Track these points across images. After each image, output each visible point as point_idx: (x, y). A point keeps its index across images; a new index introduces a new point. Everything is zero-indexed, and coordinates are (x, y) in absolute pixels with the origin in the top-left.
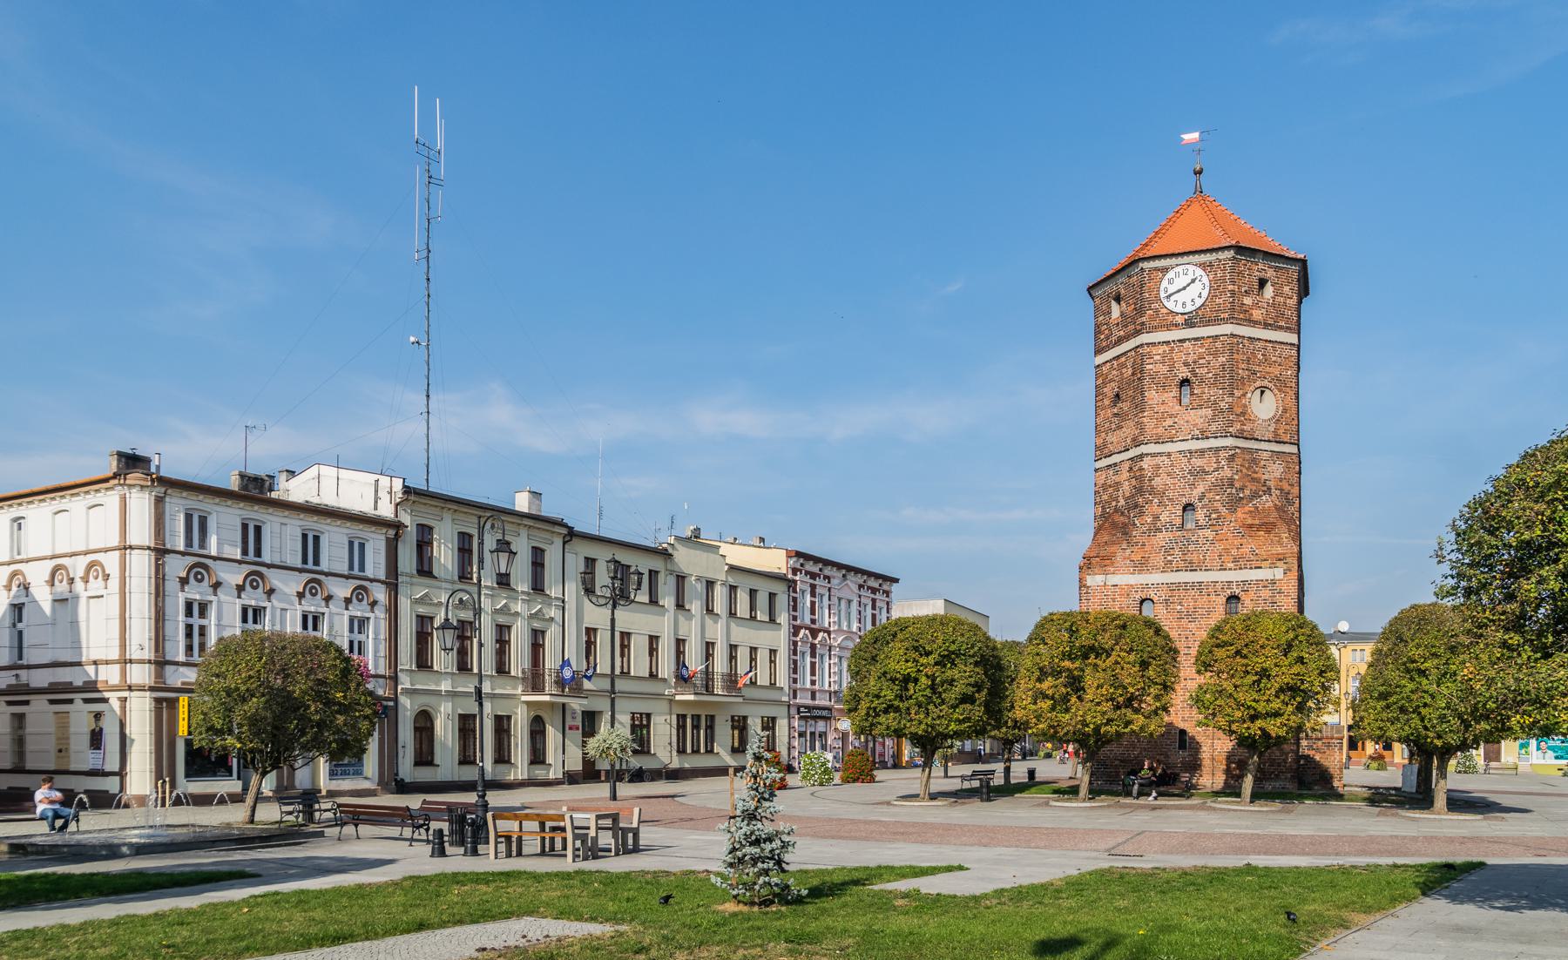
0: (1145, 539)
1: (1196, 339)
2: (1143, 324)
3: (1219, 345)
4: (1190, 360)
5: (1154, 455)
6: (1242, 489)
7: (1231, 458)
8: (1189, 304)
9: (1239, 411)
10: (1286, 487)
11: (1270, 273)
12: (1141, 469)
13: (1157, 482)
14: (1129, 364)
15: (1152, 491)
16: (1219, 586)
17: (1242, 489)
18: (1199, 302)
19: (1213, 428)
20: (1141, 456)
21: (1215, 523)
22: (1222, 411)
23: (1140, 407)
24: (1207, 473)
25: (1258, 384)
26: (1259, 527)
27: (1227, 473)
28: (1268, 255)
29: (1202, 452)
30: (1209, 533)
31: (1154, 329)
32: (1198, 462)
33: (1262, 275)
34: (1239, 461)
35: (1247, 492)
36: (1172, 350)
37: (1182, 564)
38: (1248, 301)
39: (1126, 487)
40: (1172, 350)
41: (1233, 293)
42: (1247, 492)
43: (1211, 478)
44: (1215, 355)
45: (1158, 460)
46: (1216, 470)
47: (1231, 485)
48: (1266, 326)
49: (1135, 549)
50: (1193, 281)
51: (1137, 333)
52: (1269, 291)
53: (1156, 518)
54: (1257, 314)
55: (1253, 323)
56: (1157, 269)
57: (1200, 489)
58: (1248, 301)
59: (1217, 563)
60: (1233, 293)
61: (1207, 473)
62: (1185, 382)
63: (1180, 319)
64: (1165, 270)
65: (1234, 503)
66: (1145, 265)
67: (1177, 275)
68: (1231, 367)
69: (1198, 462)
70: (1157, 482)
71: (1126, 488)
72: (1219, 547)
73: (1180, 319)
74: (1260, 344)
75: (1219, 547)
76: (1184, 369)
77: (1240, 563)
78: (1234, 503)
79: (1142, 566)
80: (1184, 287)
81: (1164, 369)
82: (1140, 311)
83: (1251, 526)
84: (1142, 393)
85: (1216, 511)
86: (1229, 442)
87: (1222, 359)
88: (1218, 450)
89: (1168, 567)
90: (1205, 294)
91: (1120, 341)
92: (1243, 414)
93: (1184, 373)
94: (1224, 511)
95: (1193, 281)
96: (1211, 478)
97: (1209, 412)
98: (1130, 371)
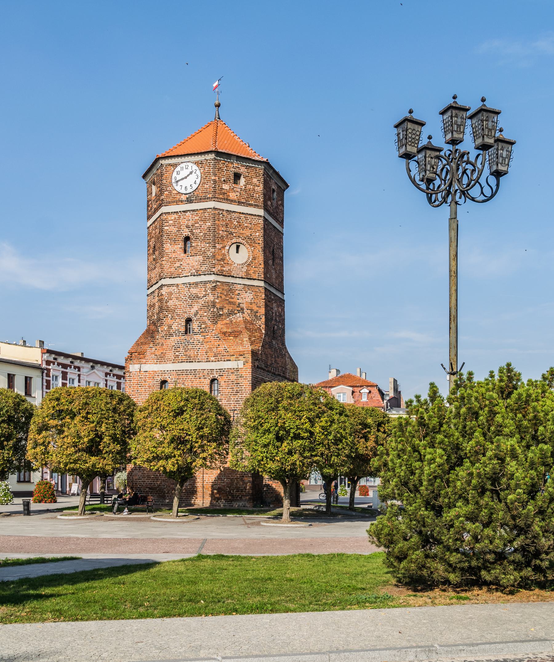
0: (162, 341)
1: (193, 211)
3: (206, 214)
4: (190, 224)
6: (222, 309)
7: (214, 288)
8: (189, 187)
9: (220, 257)
10: (255, 308)
11: (243, 170)
16: (206, 372)
17: (222, 309)
18: (195, 186)
19: (203, 269)
21: (203, 331)
22: (208, 258)
24: (199, 298)
25: (234, 240)
26: (230, 334)
27: (211, 298)
28: (239, 158)
29: (196, 284)
30: (200, 337)
31: (169, 203)
32: (194, 291)
33: (237, 170)
34: (219, 290)
35: (226, 311)
37: (184, 358)
38: (226, 187)
40: (180, 217)
41: (215, 181)
42: (226, 311)
43: (201, 301)
44: (205, 221)
45: (171, 289)
47: (214, 306)
48: (240, 203)
49: (158, 347)
50: (191, 173)
52: (242, 181)
53: (170, 327)
54: (232, 196)
55: (232, 201)
56: (170, 165)
57: (195, 308)
58: (226, 187)
59: (204, 357)
60: (215, 181)
61: (199, 298)
62: (187, 239)
63: (184, 198)
64: (175, 165)
65: (216, 318)
66: (163, 162)
67: (182, 169)
68: (214, 229)
69: (194, 291)
72: (206, 346)
73: (184, 198)
74: (236, 215)
75: (206, 346)
76: (187, 230)
77: (218, 357)
78: (216, 318)
79: (161, 359)
80: (187, 177)
81: (174, 230)
83: (225, 333)
85: (204, 323)
86: (212, 278)
87: (208, 224)
88: (206, 283)
89: (176, 359)
90: (198, 181)
92: (223, 260)
94: (209, 323)
95: (191, 173)
96: (201, 301)
97: (201, 258)
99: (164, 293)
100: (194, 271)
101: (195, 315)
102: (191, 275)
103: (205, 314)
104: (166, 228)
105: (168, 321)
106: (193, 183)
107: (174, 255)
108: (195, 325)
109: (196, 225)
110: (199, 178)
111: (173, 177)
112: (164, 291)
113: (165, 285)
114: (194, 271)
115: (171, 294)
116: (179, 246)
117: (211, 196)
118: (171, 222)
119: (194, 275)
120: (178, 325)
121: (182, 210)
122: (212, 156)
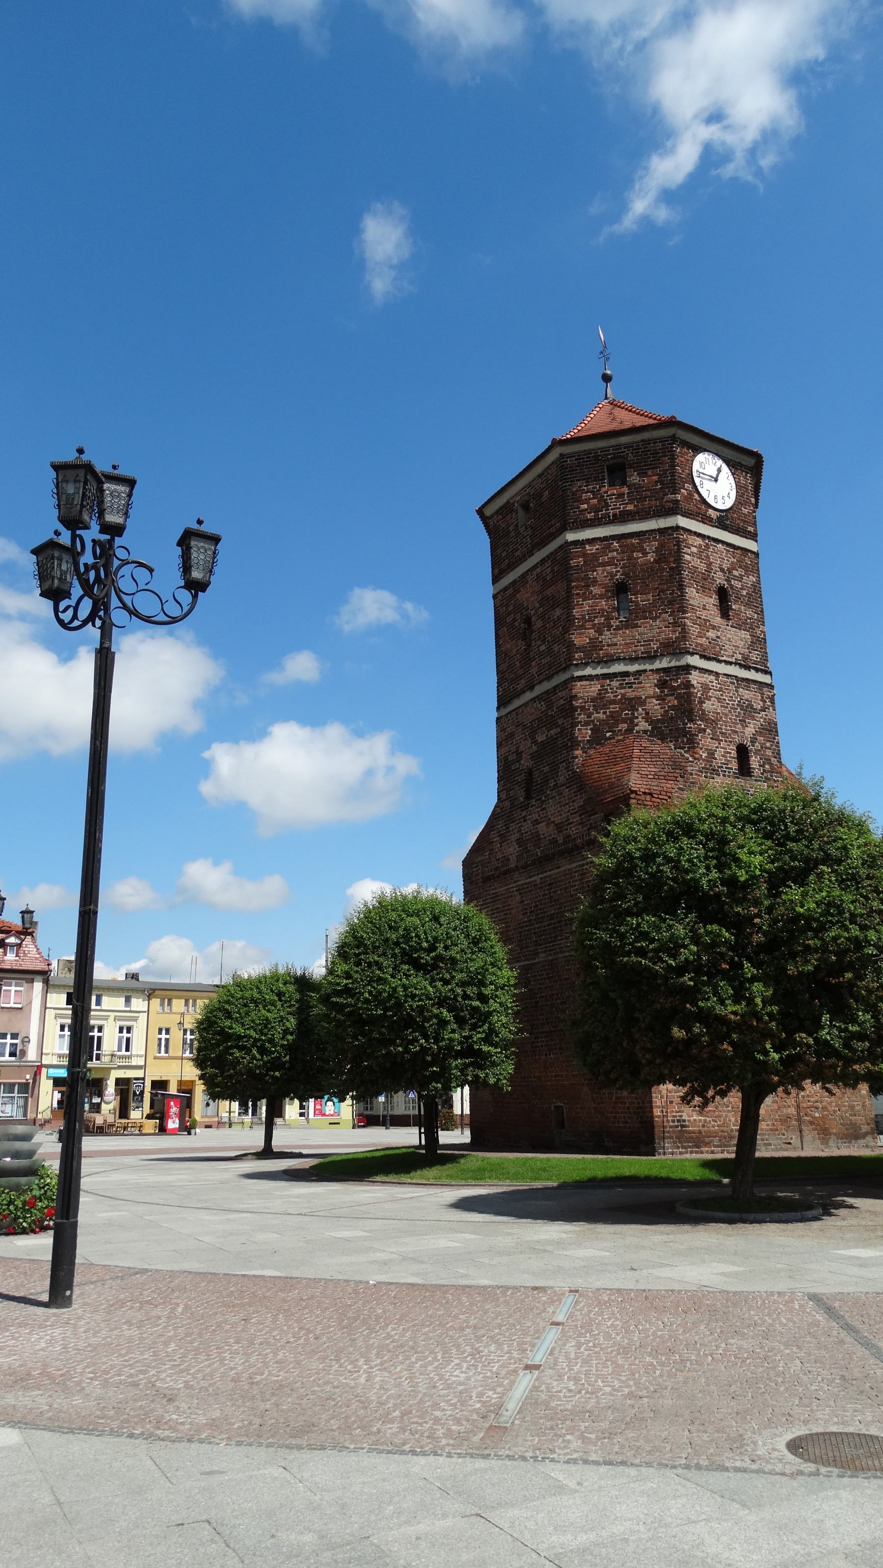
2: (677, 502)
4: (725, 567)
12: (688, 685)
13: (708, 706)
14: (651, 547)
15: (704, 717)
18: (728, 504)
20: (688, 668)
29: (747, 680)
32: (746, 694)
36: (707, 546)
39: (654, 706)
40: (707, 546)
46: (763, 709)
51: (674, 510)
53: (711, 754)
57: (750, 730)
61: (755, 711)
64: (697, 450)
70: (708, 706)
81: (702, 567)
84: (681, 587)
85: (768, 761)
93: (720, 579)
98: (651, 557)
99: (694, 682)
100: (740, 657)
101: (753, 742)
102: (736, 664)
103: (768, 744)
104: (687, 557)
105: (705, 741)
106: (726, 496)
107: (704, 615)
108: (754, 762)
109: (735, 573)
110: (734, 491)
111: (694, 470)
113: (696, 668)
114: (740, 657)
115: (706, 688)
116: (712, 601)
117: (750, 529)
118: (694, 550)
119: (741, 666)
120: (725, 754)
121: (712, 535)
122: (751, 462)
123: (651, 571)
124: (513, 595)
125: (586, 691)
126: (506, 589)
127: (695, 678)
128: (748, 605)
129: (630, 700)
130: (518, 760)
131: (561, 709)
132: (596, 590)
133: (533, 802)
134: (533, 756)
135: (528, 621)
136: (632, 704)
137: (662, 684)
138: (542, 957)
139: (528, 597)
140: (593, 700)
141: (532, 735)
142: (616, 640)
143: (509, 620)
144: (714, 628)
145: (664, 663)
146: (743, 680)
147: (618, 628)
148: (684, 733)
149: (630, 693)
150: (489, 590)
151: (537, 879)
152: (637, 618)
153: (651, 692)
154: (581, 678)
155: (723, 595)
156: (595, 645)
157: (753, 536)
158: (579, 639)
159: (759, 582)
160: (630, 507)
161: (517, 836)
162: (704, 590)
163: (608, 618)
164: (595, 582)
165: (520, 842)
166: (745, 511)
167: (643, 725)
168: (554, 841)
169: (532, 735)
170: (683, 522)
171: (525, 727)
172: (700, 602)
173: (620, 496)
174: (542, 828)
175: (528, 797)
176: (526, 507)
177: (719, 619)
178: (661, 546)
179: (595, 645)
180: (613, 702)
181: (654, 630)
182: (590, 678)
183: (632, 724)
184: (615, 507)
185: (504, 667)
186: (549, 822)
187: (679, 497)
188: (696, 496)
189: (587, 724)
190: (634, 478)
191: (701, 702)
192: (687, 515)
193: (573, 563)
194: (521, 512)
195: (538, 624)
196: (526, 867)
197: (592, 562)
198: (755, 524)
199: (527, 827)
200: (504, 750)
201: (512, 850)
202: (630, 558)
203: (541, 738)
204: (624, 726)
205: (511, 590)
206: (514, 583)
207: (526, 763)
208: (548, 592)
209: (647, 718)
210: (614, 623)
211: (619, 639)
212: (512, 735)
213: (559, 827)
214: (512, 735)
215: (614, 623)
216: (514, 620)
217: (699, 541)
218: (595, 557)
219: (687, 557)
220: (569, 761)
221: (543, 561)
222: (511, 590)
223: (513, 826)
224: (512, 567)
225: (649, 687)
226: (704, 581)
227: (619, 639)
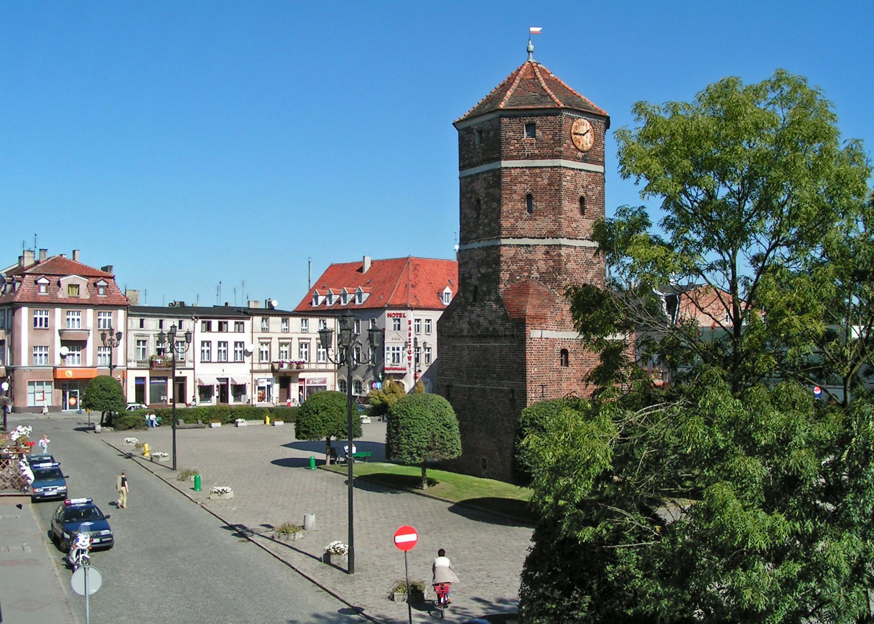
2: (561, 152)
5: (568, 246)
12: (559, 255)
13: (569, 266)
14: (546, 176)
18: (589, 146)
20: (560, 246)
23: (557, 210)
36: (576, 174)
39: (542, 266)
71: (542, 266)
76: (581, 189)
81: (572, 187)
82: (559, 142)
84: (560, 201)
91: (532, 157)
98: (546, 182)
99: (563, 254)
104: (564, 183)
112: (563, 252)
115: (569, 256)
117: (601, 159)
118: (568, 178)
123: (544, 189)
124: (473, 181)
125: (506, 253)
126: (466, 177)
127: (563, 252)
128: (595, 204)
129: (530, 260)
130: (470, 278)
131: (492, 258)
132: (515, 197)
133: (477, 304)
134: (478, 279)
135: (478, 201)
136: (531, 262)
137: (547, 253)
138: (478, 386)
139: (479, 187)
140: (511, 258)
141: (479, 267)
142: (524, 226)
143: (468, 196)
144: (575, 221)
145: (549, 241)
146: (589, 248)
147: (526, 220)
148: (555, 280)
149: (530, 257)
150: (457, 173)
151: (478, 345)
152: (536, 215)
153: (541, 257)
154: (505, 245)
155: (582, 200)
156: (513, 228)
157: (603, 163)
158: (505, 223)
159: (603, 190)
160: (536, 152)
161: (468, 319)
162: (572, 201)
163: (521, 214)
164: (515, 192)
165: (469, 323)
166: (598, 149)
167: (535, 274)
168: (488, 329)
169: (479, 267)
170: (563, 163)
171: (474, 261)
172: (570, 207)
173: (532, 144)
174: (481, 319)
175: (475, 300)
176: (480, 132)
177: (579, 216)
178: (551, 176)
179: (513, 228)
180: (521, 260)
181: (544, 223)
182: (510, 246)
183: (529, 272)
184: (529, 150)
185: (464, 222)
186: (485, 318)
187: (562, 149)
188: (572, 147)
189: (507, 271)
190: (539, 133)
191: (566, 264)
192: (566, 158)
193: (504, 180)
194: (477, 134)
195: (484, 207)
196: (472, 337)
197: (514, 181)
198: (604, 156)
199: (474, 316)
200: (462, 269)
201: (465, 326)
202: (535, 180)
203: (483, 271)
204: (526, 274)
205: (469, 179)
206: (471, 176)
207: (474, 281)
208: (491, 190)
209: (538, 270)
210: (524, 217)
211: (526, 226)
212: (466, 263)
213: (490, 322)
214: (466, 263)
215: (524, 217)
216: (471, 198)
217: (572, 172)
218: (516, 178)
219: (564, 183)
220: (497, 288)
221: (488, 172)
222: (469, 179)
223: (466, 314)
224: (472, 165)
225: (540, 255)
226: (572, 196)
227: (526, 226)
